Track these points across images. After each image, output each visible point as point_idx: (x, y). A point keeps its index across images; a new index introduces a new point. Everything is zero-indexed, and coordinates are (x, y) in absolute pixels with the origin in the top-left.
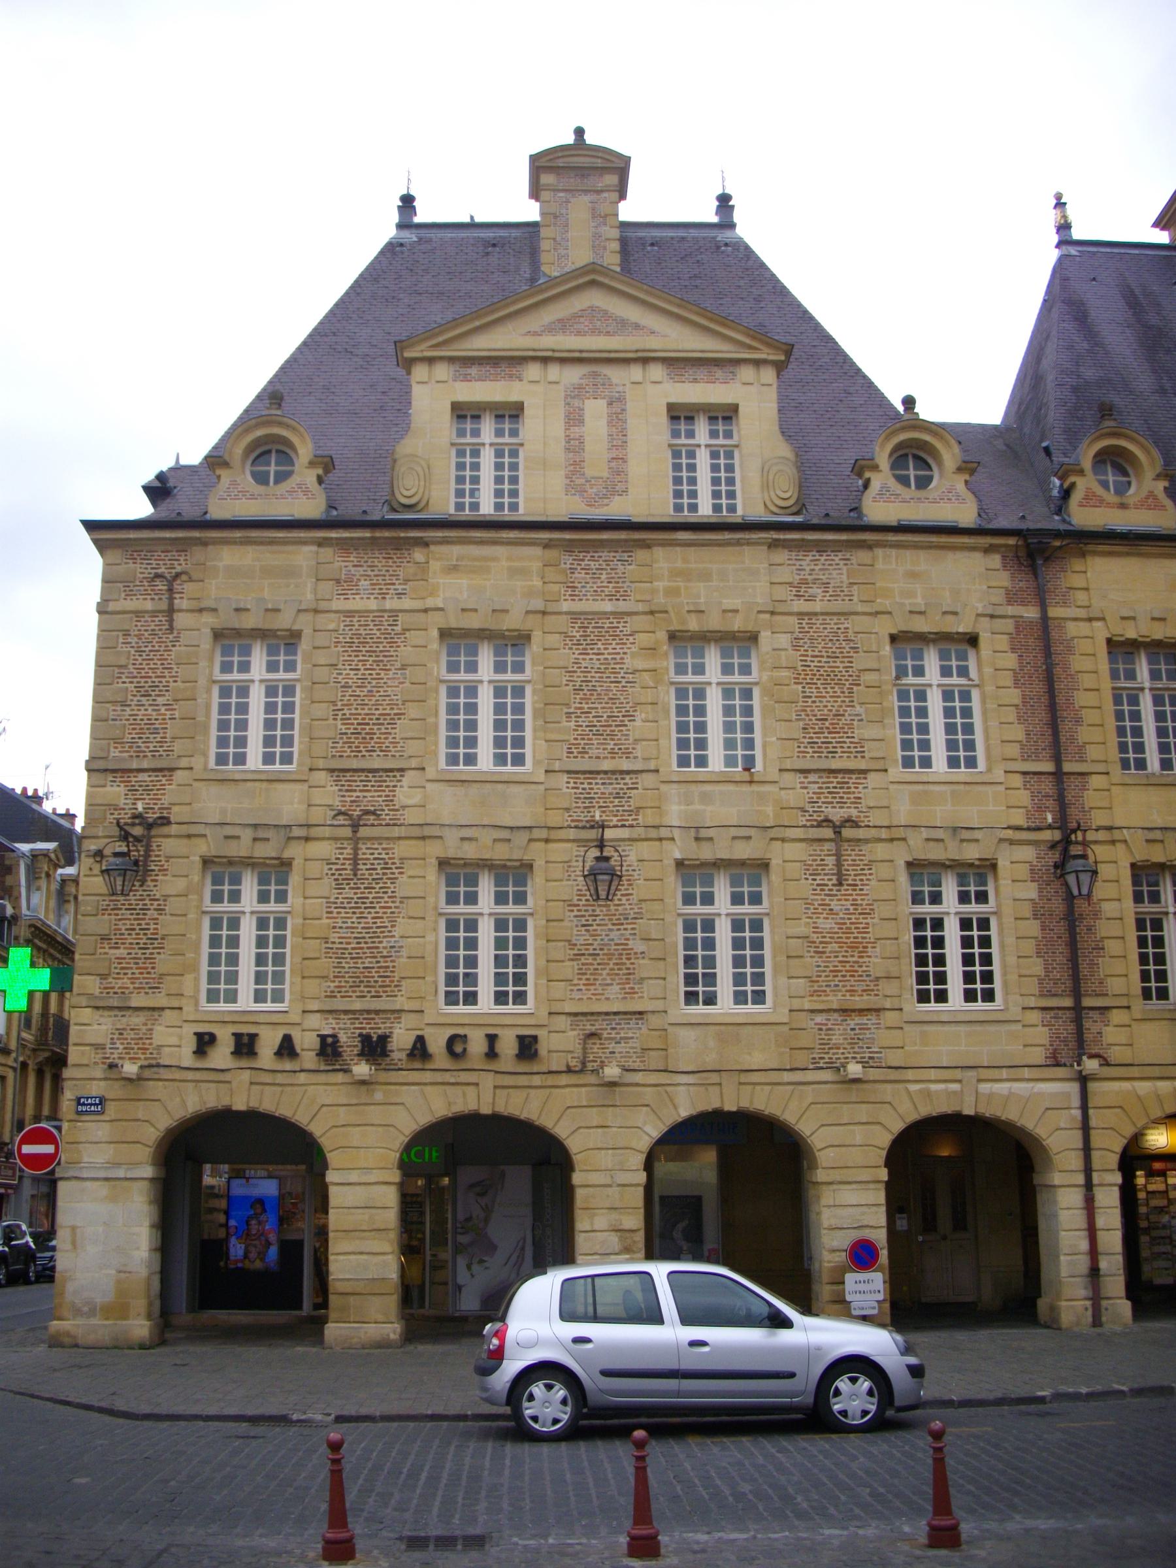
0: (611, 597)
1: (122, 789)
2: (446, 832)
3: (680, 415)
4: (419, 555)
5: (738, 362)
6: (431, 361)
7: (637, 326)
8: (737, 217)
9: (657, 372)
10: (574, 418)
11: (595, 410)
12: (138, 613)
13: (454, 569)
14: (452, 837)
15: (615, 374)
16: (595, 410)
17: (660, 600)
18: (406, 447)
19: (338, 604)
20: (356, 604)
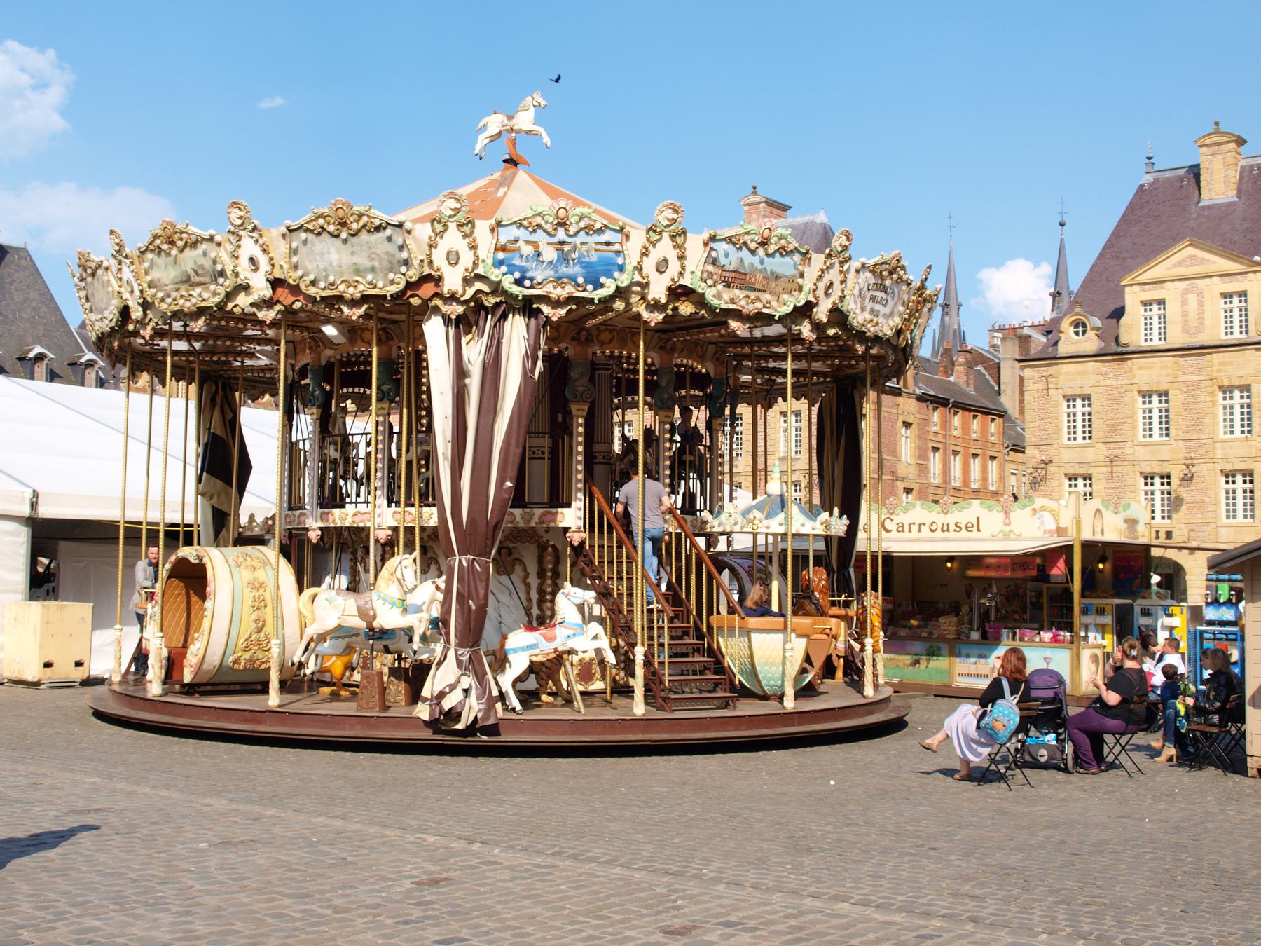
0: (1197, 374)
1: (1037, 452)
2: (1141, 463)
3: (1226, 296)
4: (1129, 362)
5: (1246, 273)
6: (1131, 285)
7: (1208, 261)
9: (1216, 279)
10: (1184, 303)
11: (1192, 298)
12: (1037, 390)
13: (1141, 368)
14: (1143, 464)
16: (1192, 298)
17: (1215, 374)
19: (1102, 383)
20: (1109, 383)
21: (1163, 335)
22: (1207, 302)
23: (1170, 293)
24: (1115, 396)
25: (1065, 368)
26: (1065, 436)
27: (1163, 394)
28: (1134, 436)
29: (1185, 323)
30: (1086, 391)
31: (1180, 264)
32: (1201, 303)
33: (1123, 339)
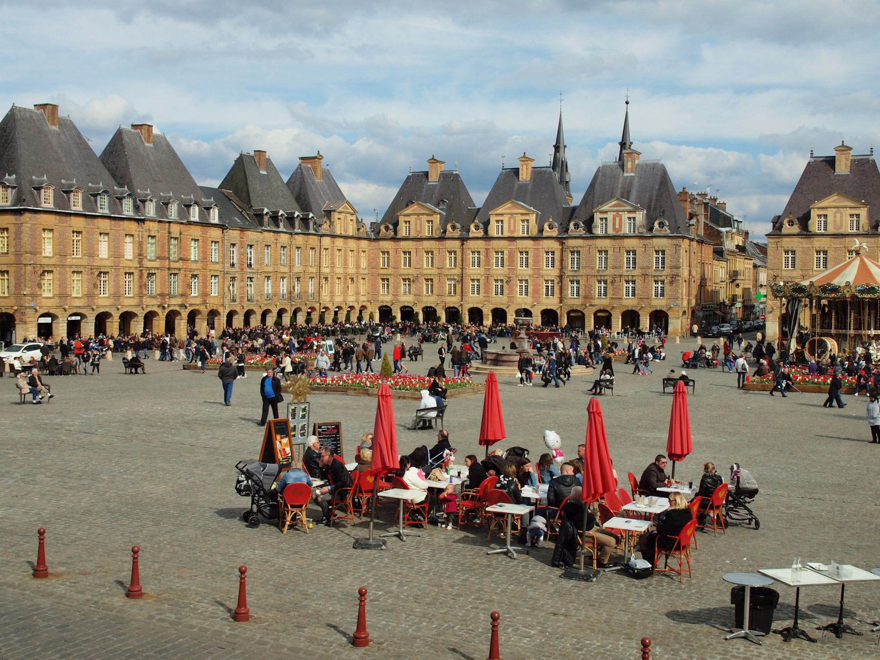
3: (852, 216)
8: (874, 153)
10: (835, 216)
11: (838, 215)
15: (842, 210)
16: (838, 215)
18: (810, 222)
21: (825, 229)
22: (844, 218)
23: (830, 213)
24: (806, 252)
25: (785, 239)
26: (784, 266)
27: (825, 252)
28: (813, 267)
29: (835, 224)
30: (794, 249)
31: (834, 201)
32: (841, 217)
33: (811, 228)
